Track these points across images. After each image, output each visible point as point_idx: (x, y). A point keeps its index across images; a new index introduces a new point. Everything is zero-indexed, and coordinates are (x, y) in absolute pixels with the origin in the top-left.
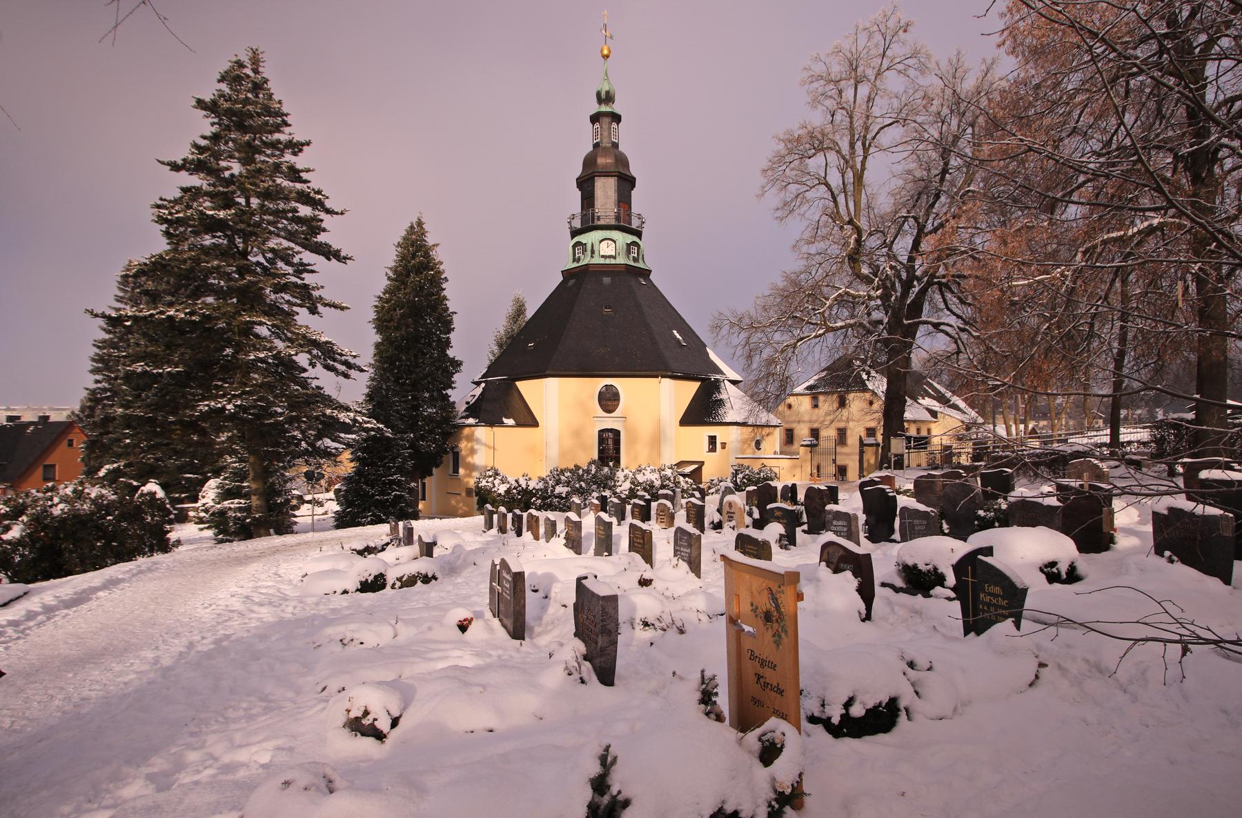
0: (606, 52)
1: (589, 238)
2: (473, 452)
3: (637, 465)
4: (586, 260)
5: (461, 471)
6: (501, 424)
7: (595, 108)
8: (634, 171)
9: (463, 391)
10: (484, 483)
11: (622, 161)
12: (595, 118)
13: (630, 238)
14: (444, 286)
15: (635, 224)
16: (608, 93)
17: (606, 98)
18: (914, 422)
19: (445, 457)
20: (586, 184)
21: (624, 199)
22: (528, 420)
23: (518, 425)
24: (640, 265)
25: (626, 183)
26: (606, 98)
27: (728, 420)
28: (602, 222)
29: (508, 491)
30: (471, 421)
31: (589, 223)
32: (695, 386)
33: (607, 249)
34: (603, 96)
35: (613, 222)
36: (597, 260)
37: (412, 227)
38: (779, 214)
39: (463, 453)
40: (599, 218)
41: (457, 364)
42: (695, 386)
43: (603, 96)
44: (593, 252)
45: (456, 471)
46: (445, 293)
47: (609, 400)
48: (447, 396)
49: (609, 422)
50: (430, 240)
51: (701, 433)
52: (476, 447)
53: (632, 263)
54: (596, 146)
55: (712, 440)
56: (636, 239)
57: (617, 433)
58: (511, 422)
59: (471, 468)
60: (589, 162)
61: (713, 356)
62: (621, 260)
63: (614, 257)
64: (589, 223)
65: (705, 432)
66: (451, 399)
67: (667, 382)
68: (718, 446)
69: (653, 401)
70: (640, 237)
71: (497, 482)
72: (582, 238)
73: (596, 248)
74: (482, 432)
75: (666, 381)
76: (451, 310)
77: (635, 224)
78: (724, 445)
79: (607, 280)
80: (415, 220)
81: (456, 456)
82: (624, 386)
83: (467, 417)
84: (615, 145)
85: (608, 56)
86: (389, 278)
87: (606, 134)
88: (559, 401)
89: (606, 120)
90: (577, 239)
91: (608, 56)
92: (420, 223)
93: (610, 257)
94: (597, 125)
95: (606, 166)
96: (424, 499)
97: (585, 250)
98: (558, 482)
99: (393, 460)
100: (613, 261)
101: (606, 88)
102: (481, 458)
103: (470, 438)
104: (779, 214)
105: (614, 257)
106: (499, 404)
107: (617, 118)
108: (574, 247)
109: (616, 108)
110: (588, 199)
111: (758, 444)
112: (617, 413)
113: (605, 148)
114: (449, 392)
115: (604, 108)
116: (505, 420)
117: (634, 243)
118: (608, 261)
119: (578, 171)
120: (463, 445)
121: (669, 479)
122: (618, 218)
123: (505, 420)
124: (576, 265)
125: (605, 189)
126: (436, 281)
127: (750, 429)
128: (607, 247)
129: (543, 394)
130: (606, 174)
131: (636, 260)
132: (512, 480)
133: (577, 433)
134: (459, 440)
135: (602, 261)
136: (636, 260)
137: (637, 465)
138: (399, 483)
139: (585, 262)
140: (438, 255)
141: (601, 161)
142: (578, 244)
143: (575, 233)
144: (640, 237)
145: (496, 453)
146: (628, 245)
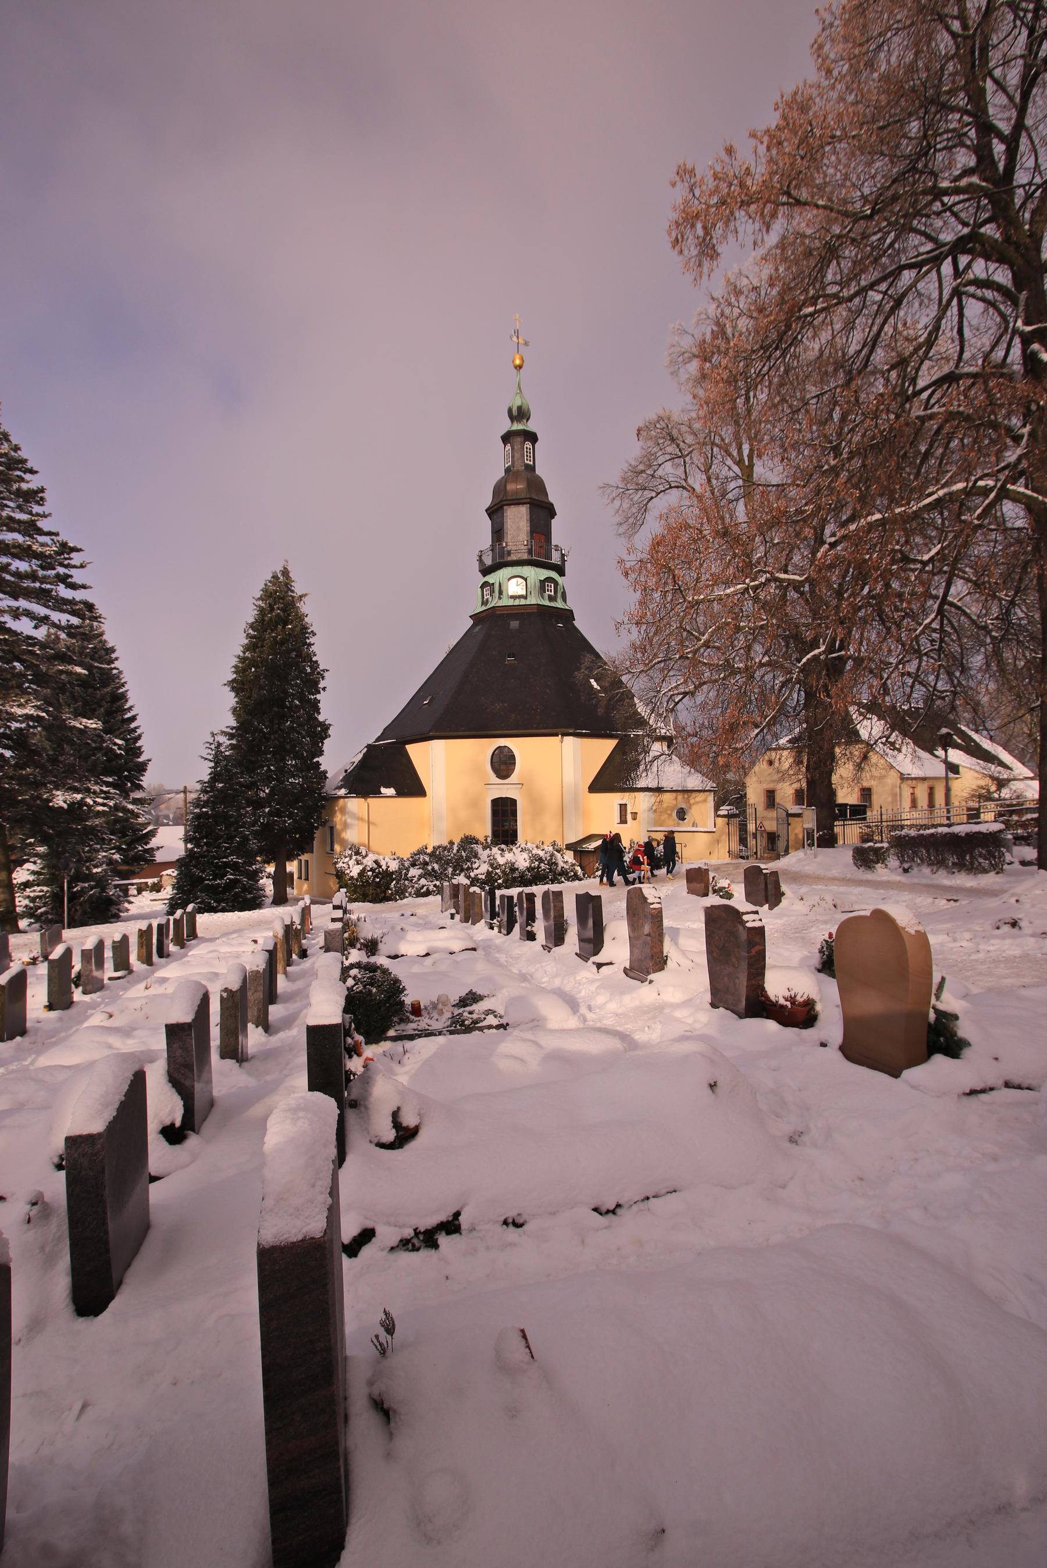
0: (518, 362)
2: (346, 826)
3: (536, 837)
4: (495, 602)
5: (337, 848)
6: (377, 793)
7: (507, 425)
9: (337, 758)
10: (340, 865)
11: (537, 485)
12: (506, 438)
13: (544, 574)
14: (311, 640)
16: (519, 408)
17: (520, 414)
18: (924, 779)
19: (317, 834)
20: (495, 512)
23: (401, 793)
24: (559, 604)
25: (542, 512)
26: (520, 414)
27: (641, 784)
28: (514, 557)
29: (362, 873)
30: (342, 792)
31: (498, 560)
32: (610, 745)
33: (515, 587)
34: (515, 412)
35: (525, 557)
36: (505, 602)
37: (275, 577)
38: (622, 530)
39: (338, 827)
40: (509, 553)
41: (325, 727)
42: (610, 745)
43: (515, 412)
44: (501, 592)
45: (332, 849)
46: (313, 648)
47: (503, 764)
48: (318, 764)
50: (298, 589)
51: (613, 800)
52: (349, 821)
53: (547, 603)
54: (508, 470)
55: (623, 807)
56: (554, 575)
57: (513, 802)
58: (391, 791)
59: (343, 843)
60: (500, 489)
61: (642, 709)
62: (533, 600)
63: (525, 597)
64: (498, 560)
65: (615, 799)
66: (322, 768)
67: (570, 742)
68: (629, 817)
69: (557, 766)
70: (562, 573)
71: (351, 863)
72: (491, 578)
73: (503, 588)
74: (355, 805)
75: (569, 740)
76: (321, 667)
77: (555, 558)
78: (635, 815)
79: (515, 624)
80: (278, 569)
81: (332, 828)
82: (526, 749)
83: (339, 788)
84: (531, 468)
86: (248, 636)
87: (517, 455)
88: (450, 766)
89: (519, 439)
92: (285, 572)
93: (520, 597)
94: (508, 447)
95: (517, 492)
96: (307, 879)
97: (492, 592)
98: (413, 865)
99: (230, 838)
100: (523, 602)
101: (518, 402)
102: (352, 835)
103: (343, 811)
104: (622, 530)
105: (525, 597)
106: (387, 769)
107: (532, 437)
108: (482, 587)
109: (531, 426)
110: (498, 533)
111: (682, 814)
112: (514, 778)
113: (518, 471)
114: (320, 759)
116: (383, 790)
117: (549, 579)
118: (517, 602)
119: (488, 500)
120: (338, 818)
121: (541, 860)
122: (530, 552)
123: (383, 790)
124: (484, 608)
125: (518, 520)
126: (302, 634)
127: (674, 794)
128: (516, 586)
129: (434, 759)
130: (517, 502)
131: (551, 599)
132: (369, 862)
133: (474, 803)
134: (333, 813)
135: (511, 602)
136: (551, 599)
137: (536, 837)
138: (235, 866)
140: (305, 607)
141: (511, 487)
142: (485, 584)
143: (486, 571)
144: (562, 573)
145: (376, 829)
146: (543, 583)
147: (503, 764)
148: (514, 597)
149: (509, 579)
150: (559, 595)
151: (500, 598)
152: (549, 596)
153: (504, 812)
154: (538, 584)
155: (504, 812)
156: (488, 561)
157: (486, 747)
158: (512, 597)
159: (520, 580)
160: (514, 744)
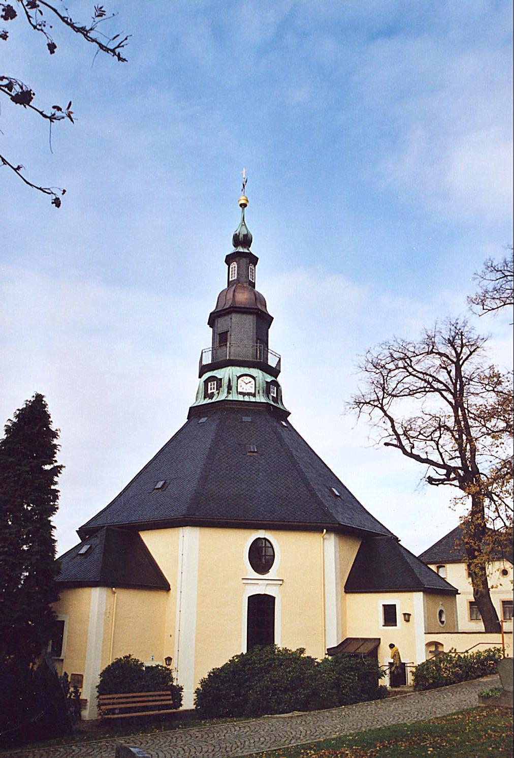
0: (243, 202)
1: (223, 373)
7: (231, 249)
8: (270, 310)
12: (229, 259)
13: (269, 379)
15: (272, 362)
16: (246, 236)
21: (262, 339)
22: (154, 581)
33: (246, 385)
36: (234, 397)
44: (230, 388)
47: (261, 558)
49: (261, 589)
56: (274, 379)
62: (260, 398)
72: (218, 373)
73: (234, 384)
85: (243, 206)
87: (244, 273)
89: (244, 261)
90: (206, 376)
91: (243, 206)
93: (249, 394)
94: (234, 265)
97: (219, 386)
100: (252, 399)
105: (254, 395)
107: (254, 260)
108: (206, 382)
109: (253, 249)
112: (272, 573)
115: (241, 249)
118: (247, 399)
124: (208, 401)
128: (246, 385)
135: (241, 398)
136: (275, 400)
139: (222, 397)
147: (261, 558)
148: (244, 394)
149: (239, 377)
150: (279, 398)
151: (229, 393)
152: (273, 397)
153: (261, 611)
154: (265, 385)
155: (261, 611)
156: (207, 360)
157: (241, 541)
158: (241, 393)
159: (251, 379)
160: (272, 536)
